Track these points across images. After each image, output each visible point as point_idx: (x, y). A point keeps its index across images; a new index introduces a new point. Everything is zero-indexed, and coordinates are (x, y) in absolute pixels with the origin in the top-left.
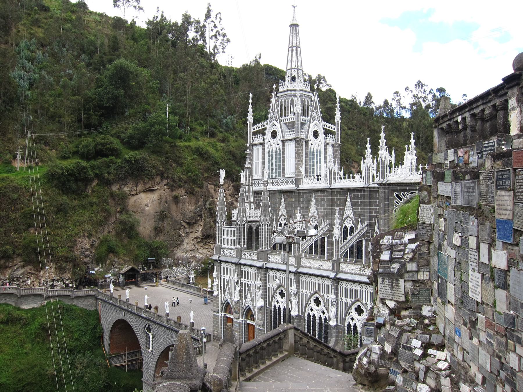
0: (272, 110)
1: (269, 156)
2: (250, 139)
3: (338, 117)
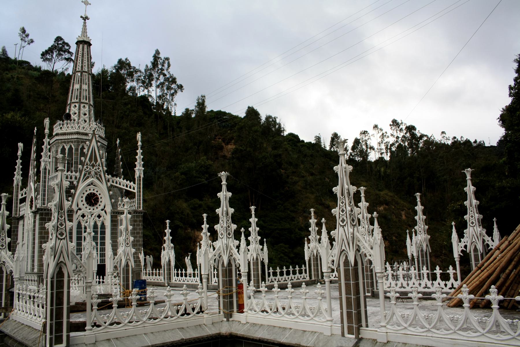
3: (139, 170)
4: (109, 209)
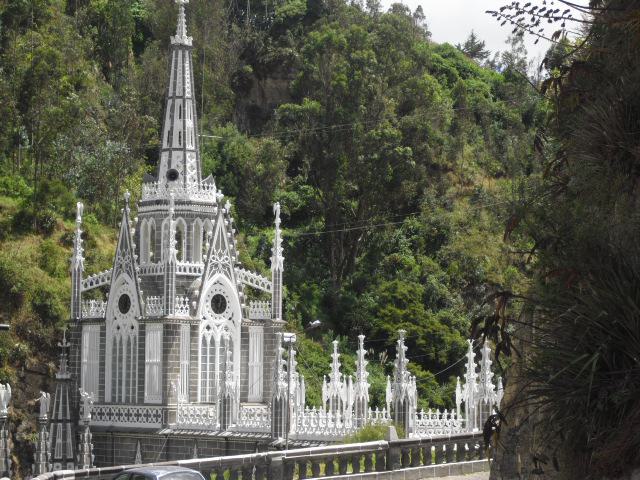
1: (114, 351)
4: (239, 318)
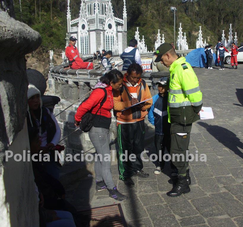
0: (82, 11)
1: (81, 40)
2: (69, 30)
3: (125, 15)
4: (115, 30)
